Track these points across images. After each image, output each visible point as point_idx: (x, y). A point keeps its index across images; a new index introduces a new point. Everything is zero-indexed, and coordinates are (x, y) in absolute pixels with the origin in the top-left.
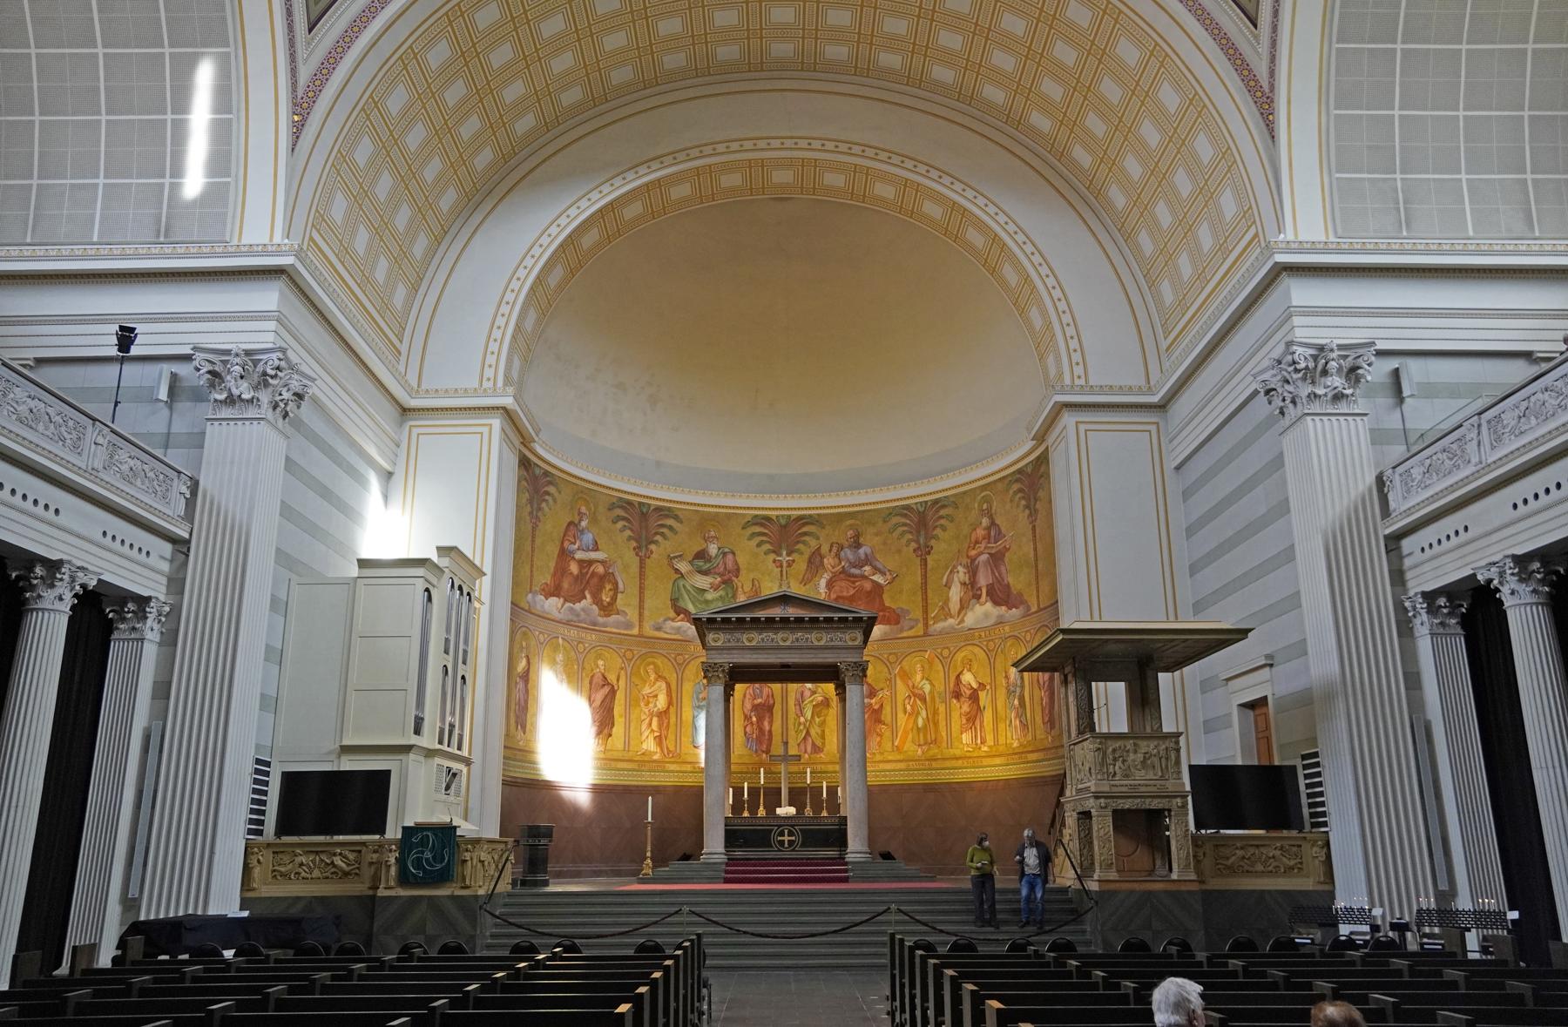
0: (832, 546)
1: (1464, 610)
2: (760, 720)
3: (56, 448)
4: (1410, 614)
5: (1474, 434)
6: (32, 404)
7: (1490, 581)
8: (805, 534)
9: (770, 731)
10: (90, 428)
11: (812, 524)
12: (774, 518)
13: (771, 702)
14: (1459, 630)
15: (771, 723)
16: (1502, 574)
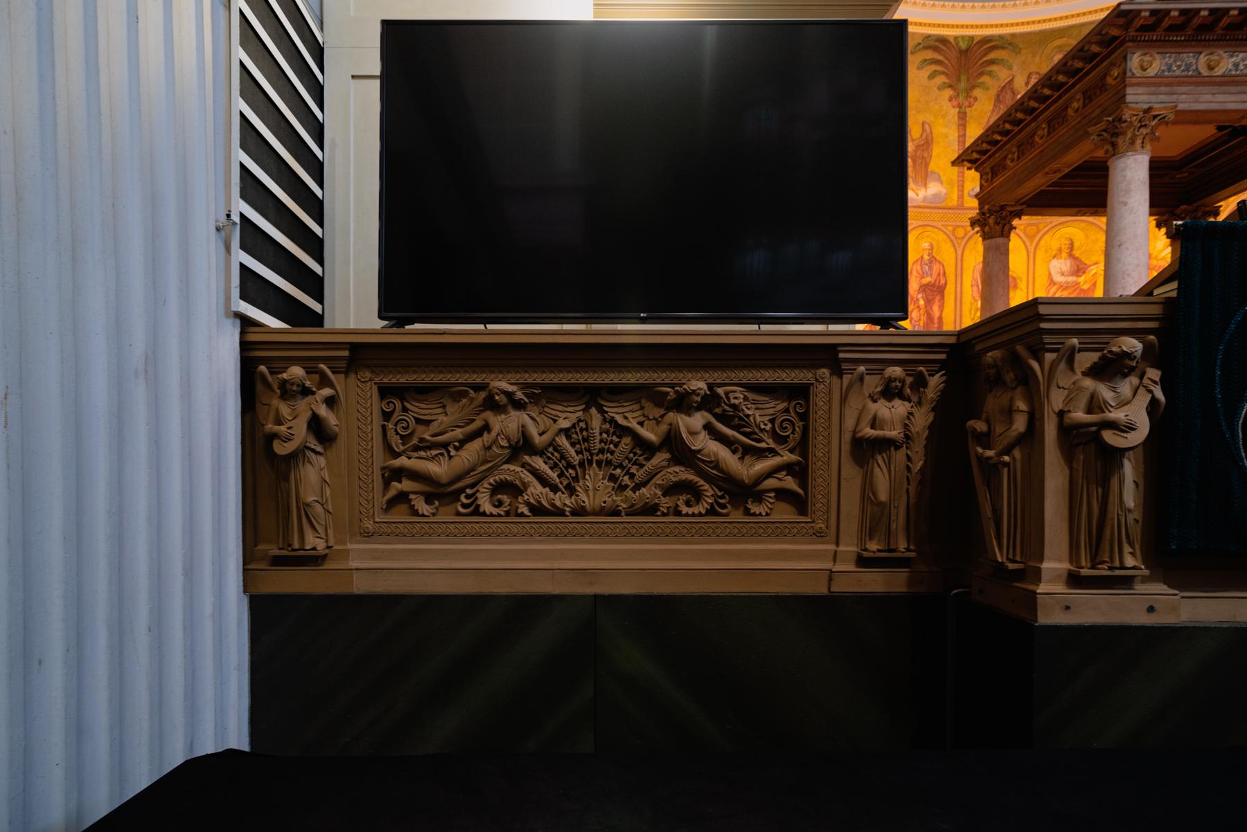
0: (1029, 77)
2: (929, 302)
8: (992, 62)
9: (940, 318)
11: (1003, 48)
12: (952, 40)
13: (943, 282)
15: (942, 307)
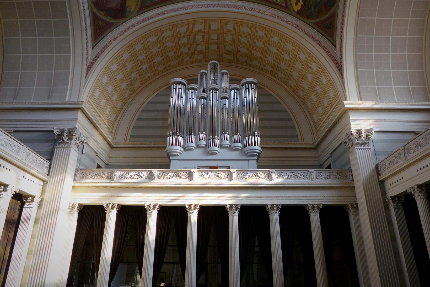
1: (403, 202)
3: (12, 153)
4: (388, 203)
5: (403, 152)
6: (5, 140)
7: (411, 192)
10: (22, 148)
14: (401, 207)
16: (414, 190)
